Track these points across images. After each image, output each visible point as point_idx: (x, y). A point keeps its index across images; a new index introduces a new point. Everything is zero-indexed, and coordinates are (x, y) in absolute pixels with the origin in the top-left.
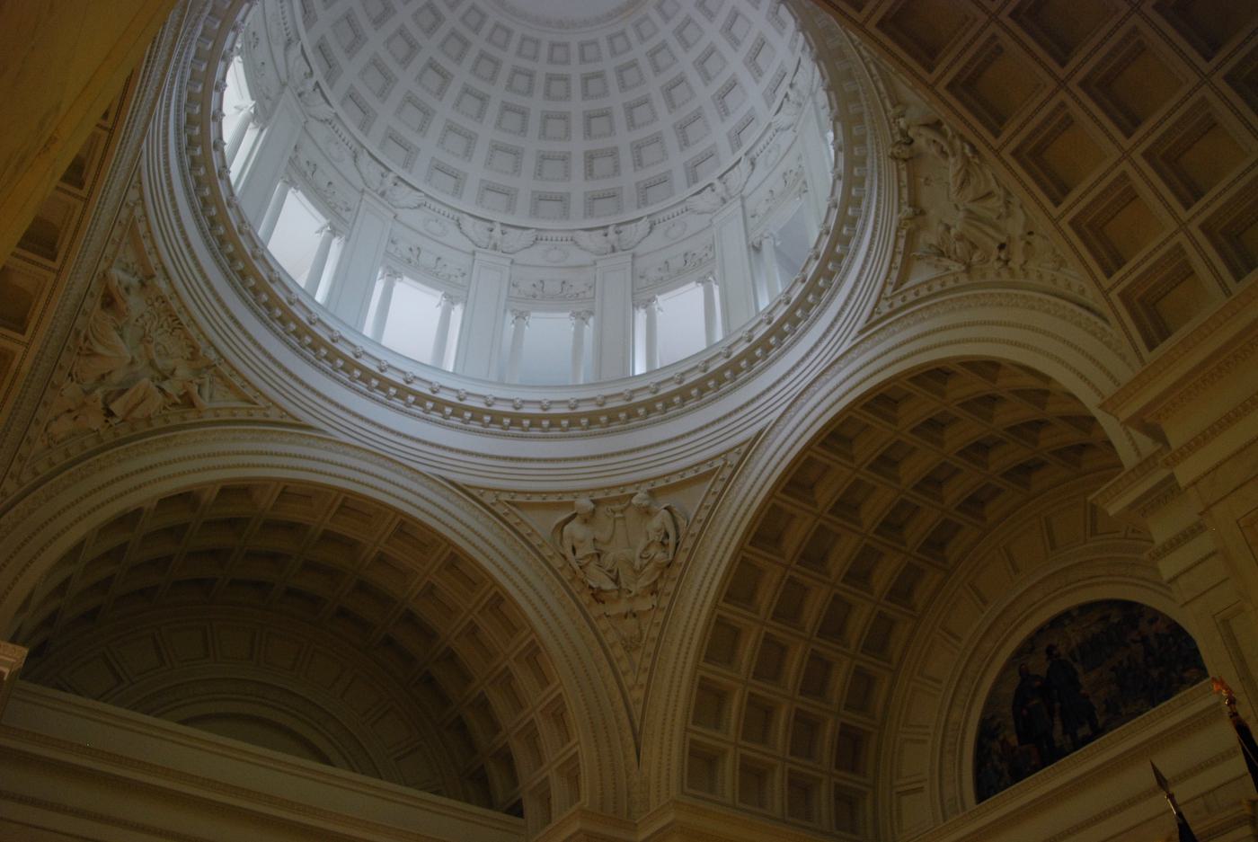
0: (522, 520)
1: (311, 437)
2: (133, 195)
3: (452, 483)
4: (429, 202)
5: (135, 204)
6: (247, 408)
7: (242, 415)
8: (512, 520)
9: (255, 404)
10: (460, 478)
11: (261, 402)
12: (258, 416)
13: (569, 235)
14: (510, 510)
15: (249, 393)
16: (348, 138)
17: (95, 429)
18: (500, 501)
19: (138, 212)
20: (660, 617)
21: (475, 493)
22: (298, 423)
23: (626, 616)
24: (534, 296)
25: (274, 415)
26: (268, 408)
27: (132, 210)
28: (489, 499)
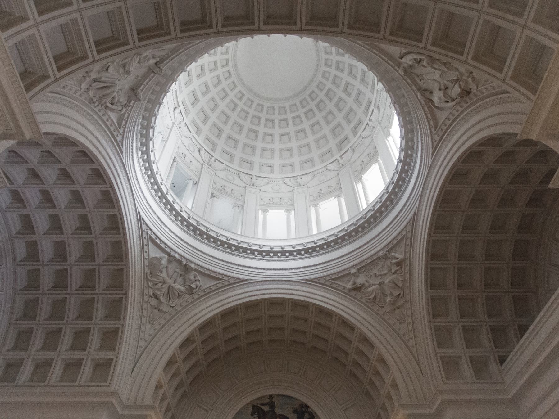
0: (148, 245)
3: (139, 213)
7: (112, 128)
8: (145, 241)
9: (120, 128)
10: (143, 215)
13: (200, 147)
18: (147, 232)
20: (168, 317)
22: (121, 146)
23: (155, 308)
24: (270, 204)
28: (144, 227)
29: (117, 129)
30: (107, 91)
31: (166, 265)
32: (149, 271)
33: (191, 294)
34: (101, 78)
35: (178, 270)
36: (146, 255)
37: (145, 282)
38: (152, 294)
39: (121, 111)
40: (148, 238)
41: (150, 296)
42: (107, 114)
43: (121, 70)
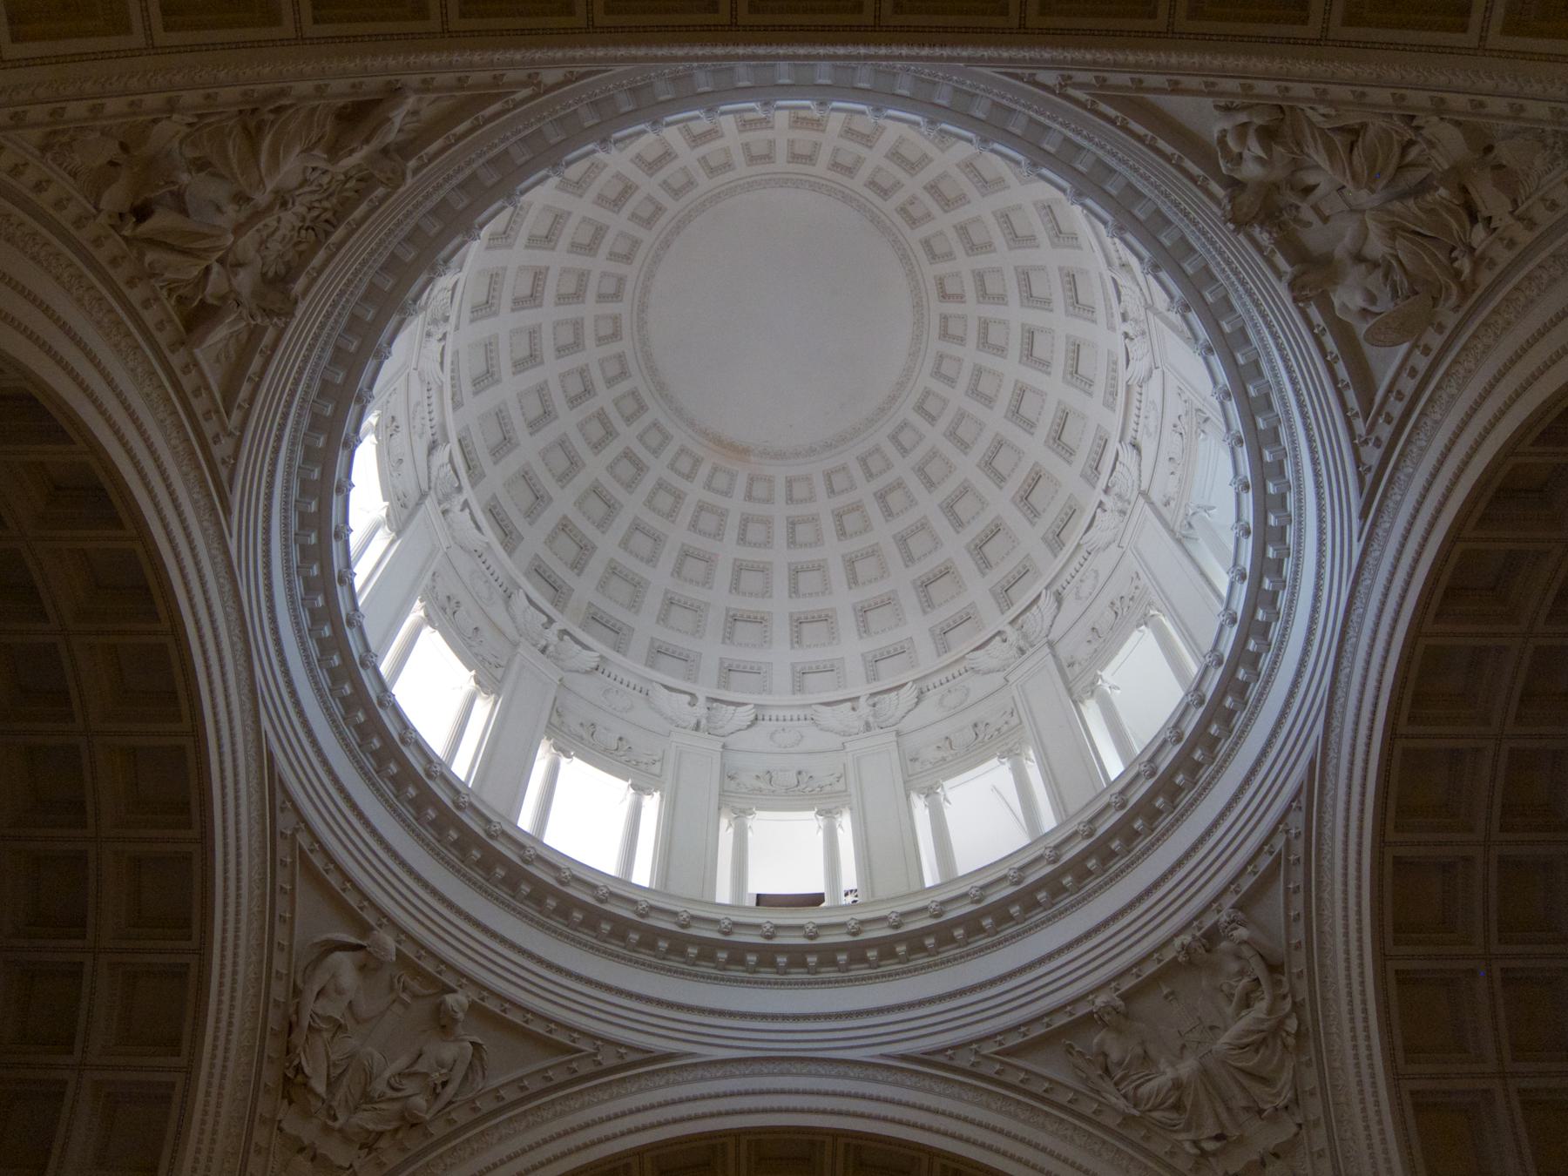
0: (1389, 390)
1: (1323, 769)
2: (965, 1060)
4: (1128, 439)
5: (976, 1052)
6: (1287, 872)
9: (1279, 854)
11: (1279, 843)
12: (1299, 847)
14: (1378, 413)
15: (1265, 862)
16: (1075, 564)
17: (1294, 1129)
18: (1370, 430)
19: (989, 1049)
21: (1369, 478)
25: (1297, 821)
26: (1287, 832)
27: (986, 1057)
28: (1372, 456)
29: (1287, 861)
30: (1251, 1062)
31: (1355, 273)
32: (1438, 309)
33: (1292, 108)
34: (1247, 1109)
35: (1307, 213)
36: (1422, 363)
37: (1486, 278)
38: (1480, 227)
39: (1245, 942)
40: (1378, 413)
41: (1495, 229)
42: (1289, 944)
43: (1188, 1102)
